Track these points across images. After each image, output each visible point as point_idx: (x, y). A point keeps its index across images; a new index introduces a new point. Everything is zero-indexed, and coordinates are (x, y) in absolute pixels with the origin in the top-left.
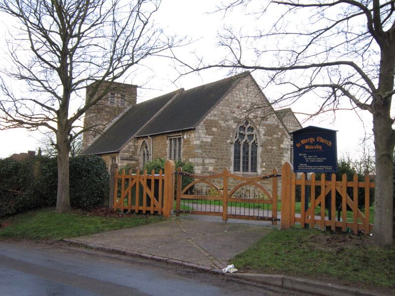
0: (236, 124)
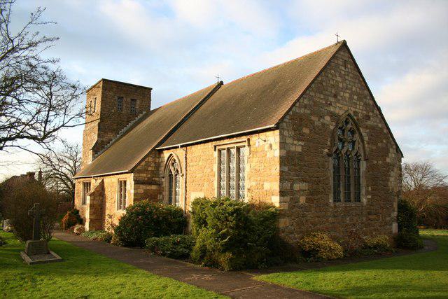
0: (334, 124)
